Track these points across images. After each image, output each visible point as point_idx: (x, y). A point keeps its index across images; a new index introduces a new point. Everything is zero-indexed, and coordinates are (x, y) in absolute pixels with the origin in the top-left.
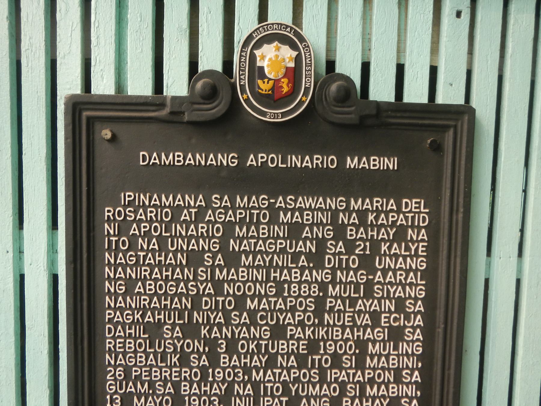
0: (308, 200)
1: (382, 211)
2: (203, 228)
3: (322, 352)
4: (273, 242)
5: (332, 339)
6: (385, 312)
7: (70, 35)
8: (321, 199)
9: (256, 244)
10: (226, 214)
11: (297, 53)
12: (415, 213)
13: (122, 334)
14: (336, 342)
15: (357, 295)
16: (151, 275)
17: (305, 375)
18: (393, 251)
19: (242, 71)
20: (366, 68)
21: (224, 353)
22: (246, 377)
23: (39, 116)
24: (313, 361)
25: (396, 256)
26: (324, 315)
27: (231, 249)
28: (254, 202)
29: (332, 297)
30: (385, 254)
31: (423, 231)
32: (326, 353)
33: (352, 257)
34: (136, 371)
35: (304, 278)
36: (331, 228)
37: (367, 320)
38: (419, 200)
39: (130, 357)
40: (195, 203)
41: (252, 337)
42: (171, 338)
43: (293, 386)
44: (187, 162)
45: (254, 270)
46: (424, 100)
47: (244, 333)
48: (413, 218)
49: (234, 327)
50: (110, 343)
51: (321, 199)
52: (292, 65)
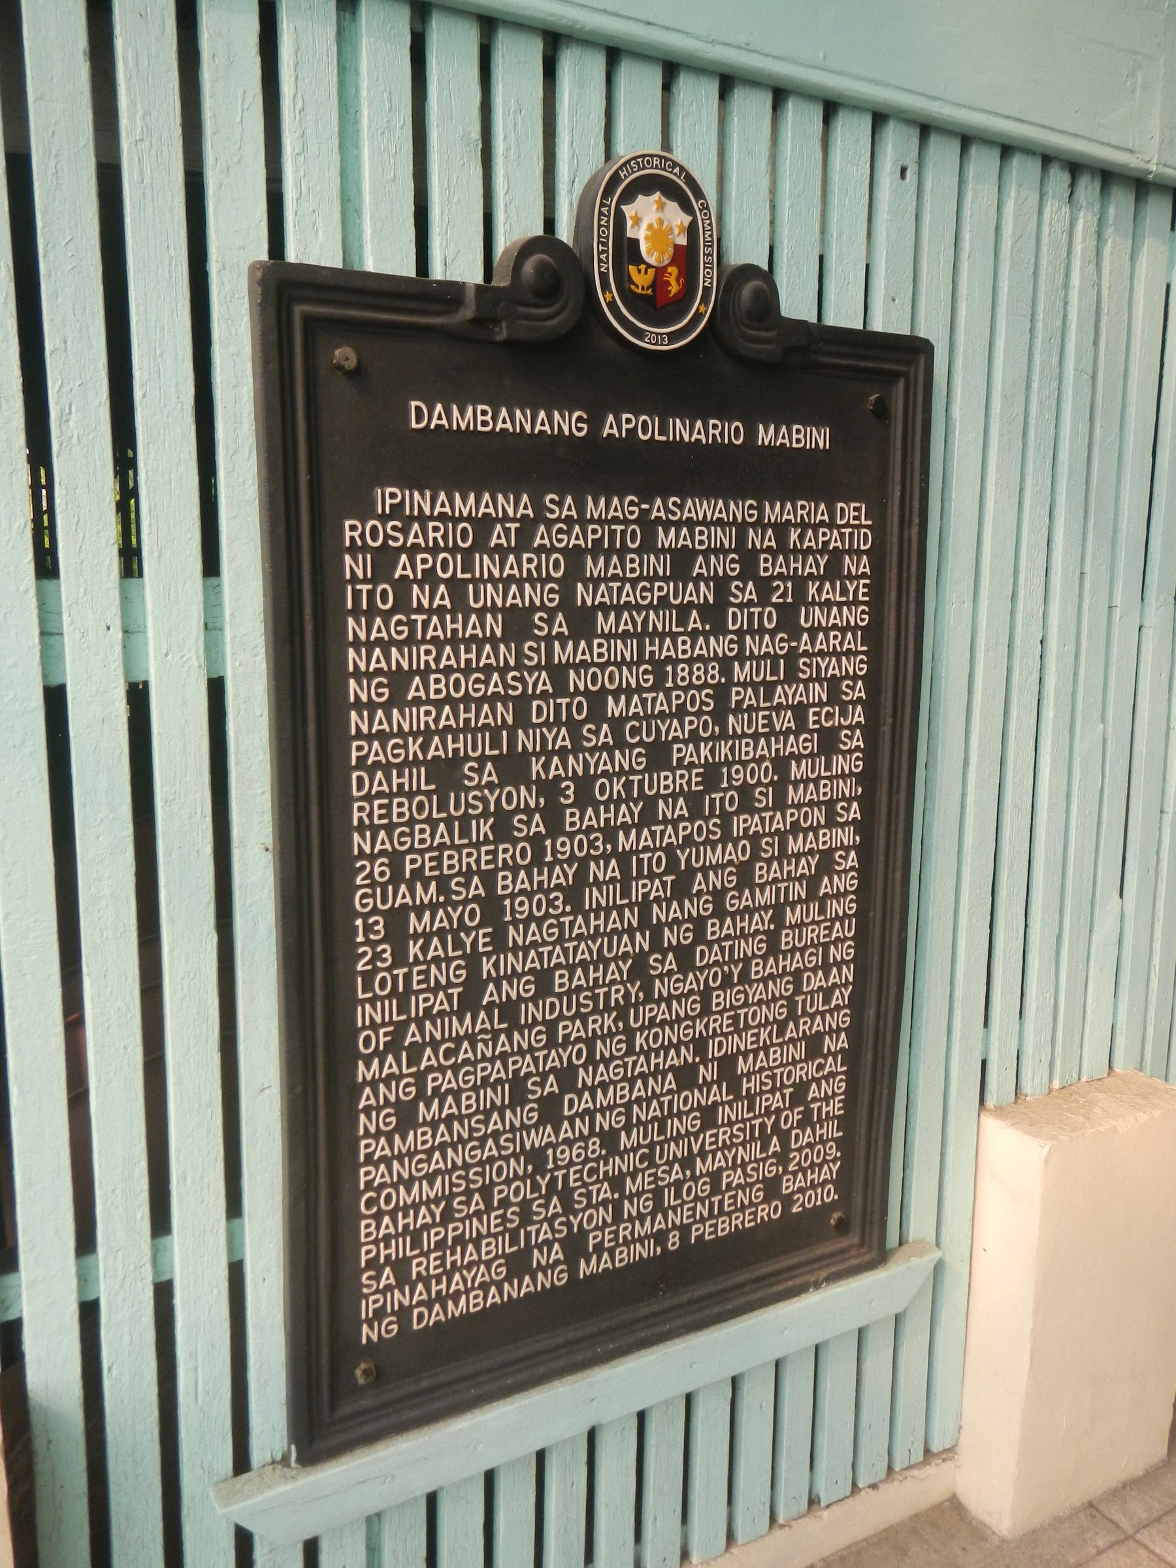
1: (809, 525)
2: (530, 561)
3: (725, 785)
5: (741, 762)
6: (814, 705)
7: (238, 119)
10: (568, 533)
11: (690, 218)
12: (854, 526)
13: (385, 788)
15: (775, 678)
16: (437, 660)
22: (609, 847)
23: (173, 305)
24: (712, 801)
25: (828, 604)
27: (579, 603)
28: (616, 510)
29: (739, 684)
30: (814, 603)
32: (731, 787)
37: (786, 720)
38: (858, 505)
39: (402, 834)
40: (515, 512)
42: (478, 787)
43: (683, 853)
44: (500, 425)
45: (619, 641)
48: (851, 535)
50: (361, 809)
52: (682, 241)
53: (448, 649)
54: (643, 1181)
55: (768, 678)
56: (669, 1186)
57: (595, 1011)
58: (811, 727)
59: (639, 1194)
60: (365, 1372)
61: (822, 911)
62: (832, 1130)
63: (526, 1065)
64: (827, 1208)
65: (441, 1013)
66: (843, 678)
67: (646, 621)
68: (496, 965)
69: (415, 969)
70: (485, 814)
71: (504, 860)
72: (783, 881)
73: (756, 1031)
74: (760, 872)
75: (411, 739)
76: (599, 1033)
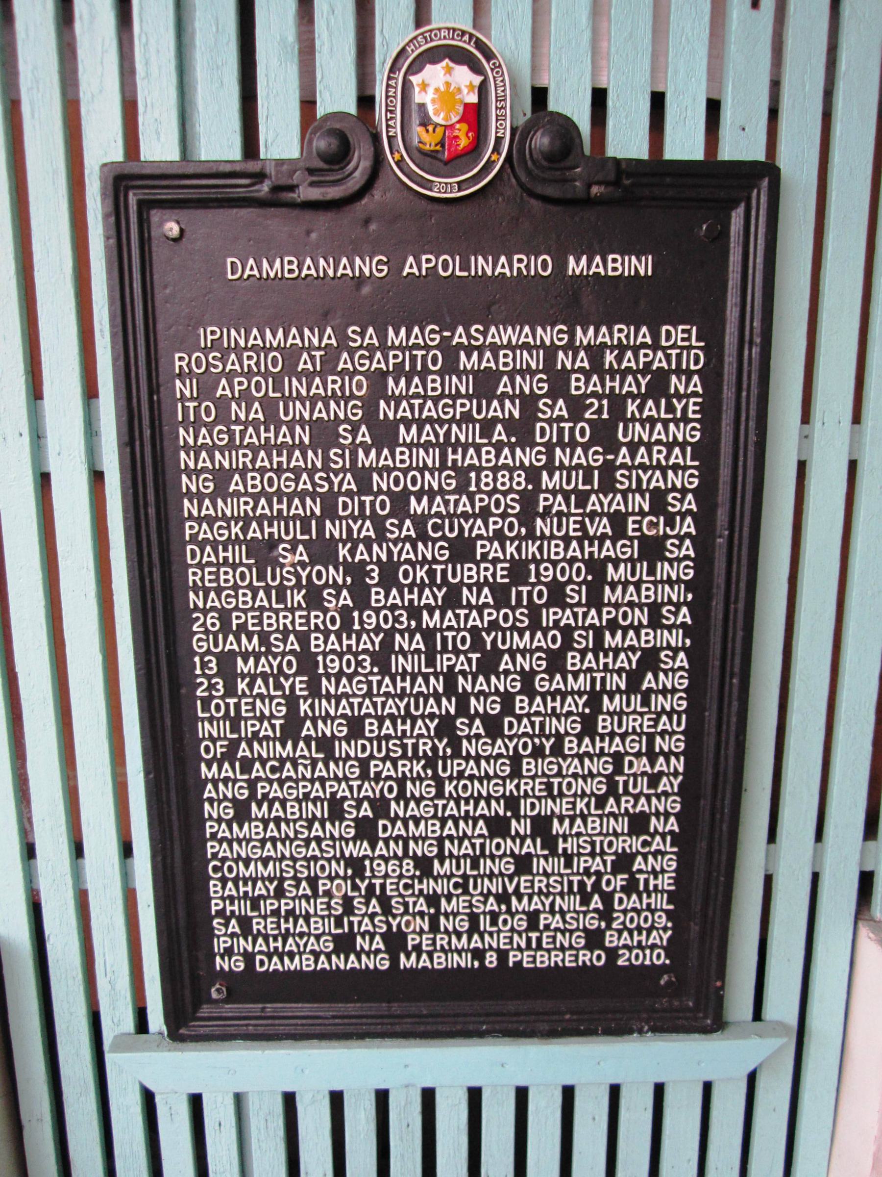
0: (505, 330)
1: (628, 347)
2: (334, 382)
3: (533, 579)
4: (450, 402)
5: (549, 560)
6: (633, 514)
8: (527, 329)
9: (422, 407)
10: (371, 358)
13: (213, 559)
14: (554, 563)
15: (588, 487)
16: (253, 461)
17: (506, 618)
18: (646, 413)
19: (391, 112)
20: (599, 97)
21: (375, 585)
22: (413, 623)
24: (519, 594)
25: (652, 421)
26: (534, 521)
28: (416, 337)
29: (547, 491)
30: (633, 419)
31: (696, 378)
32: (539, 582)
33: (580, 425)
34: (238, 618)
35: (502, 461)
36: (545, 377)
37: (604, 526)
38: (688, 327)
39: (228, 596)
40: (320, 341)
41: (420, 558)
44: (305, 272)
46: (697, 154)
47: (408, 553)
48: (679, 356)
49: (390, 544)
51: (527, 329)
52: (473, 99)
53: (262, 454)
54: (458, 904)
55: (580, 487)
56: (484, 913)
57: (404, 756)
58: (630, 533)
59: (455, 914)
60: (218, 990)
61: (646, 702)
62: (661, 902)
63: (343, 791)
64: (655, 971)
65: (267, 738)
66: (668, 491)
67: (448, 434)
68: (312, 707)
69: (243, 701)
70: (299, 586)
71: (316, 624)
72: (598, 671)
73: (572, 800)
74: (572, 660)
75: (233, 523)
76: (409, 775)
